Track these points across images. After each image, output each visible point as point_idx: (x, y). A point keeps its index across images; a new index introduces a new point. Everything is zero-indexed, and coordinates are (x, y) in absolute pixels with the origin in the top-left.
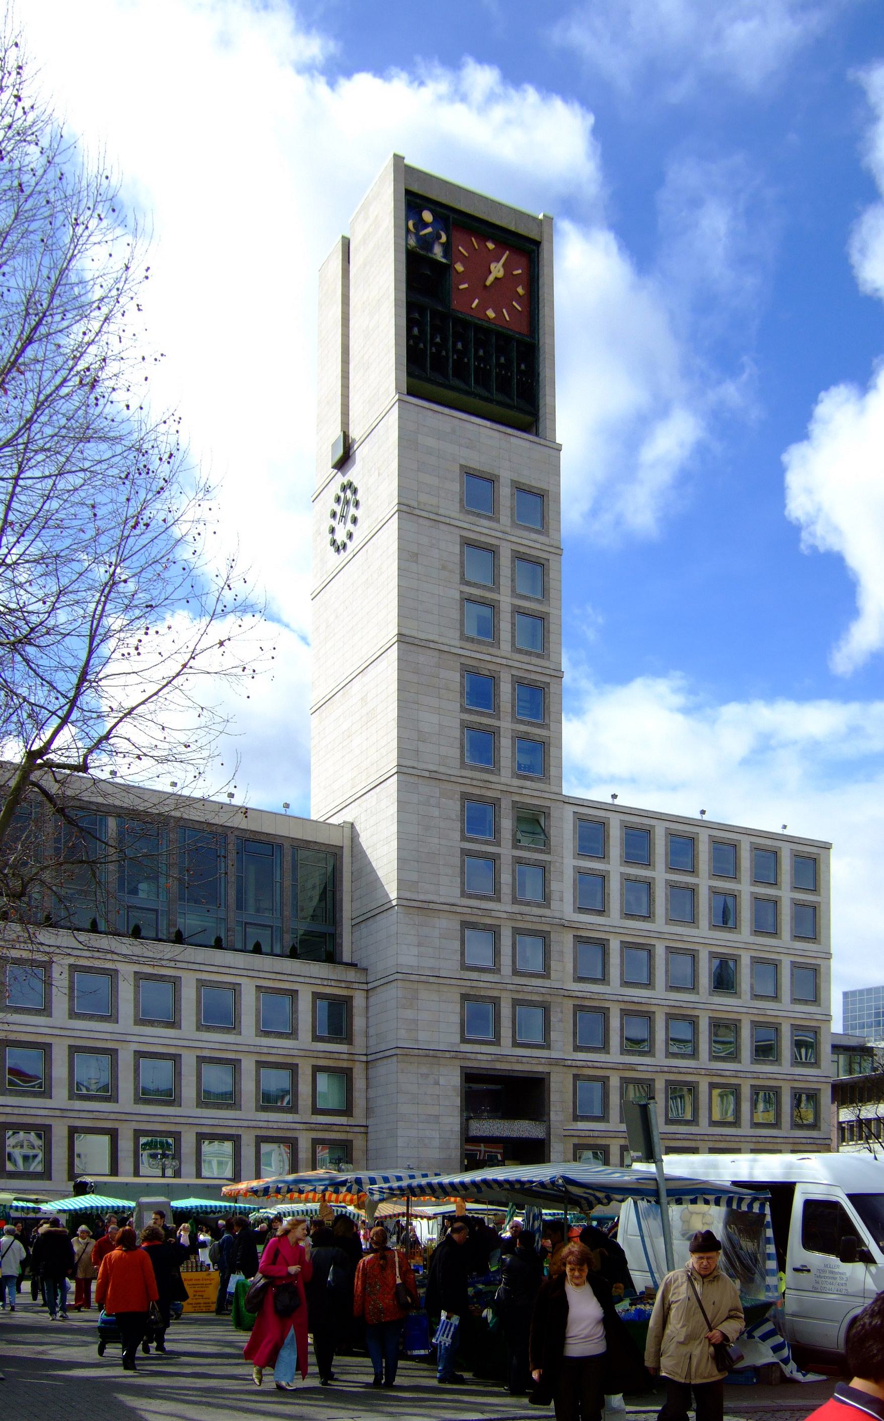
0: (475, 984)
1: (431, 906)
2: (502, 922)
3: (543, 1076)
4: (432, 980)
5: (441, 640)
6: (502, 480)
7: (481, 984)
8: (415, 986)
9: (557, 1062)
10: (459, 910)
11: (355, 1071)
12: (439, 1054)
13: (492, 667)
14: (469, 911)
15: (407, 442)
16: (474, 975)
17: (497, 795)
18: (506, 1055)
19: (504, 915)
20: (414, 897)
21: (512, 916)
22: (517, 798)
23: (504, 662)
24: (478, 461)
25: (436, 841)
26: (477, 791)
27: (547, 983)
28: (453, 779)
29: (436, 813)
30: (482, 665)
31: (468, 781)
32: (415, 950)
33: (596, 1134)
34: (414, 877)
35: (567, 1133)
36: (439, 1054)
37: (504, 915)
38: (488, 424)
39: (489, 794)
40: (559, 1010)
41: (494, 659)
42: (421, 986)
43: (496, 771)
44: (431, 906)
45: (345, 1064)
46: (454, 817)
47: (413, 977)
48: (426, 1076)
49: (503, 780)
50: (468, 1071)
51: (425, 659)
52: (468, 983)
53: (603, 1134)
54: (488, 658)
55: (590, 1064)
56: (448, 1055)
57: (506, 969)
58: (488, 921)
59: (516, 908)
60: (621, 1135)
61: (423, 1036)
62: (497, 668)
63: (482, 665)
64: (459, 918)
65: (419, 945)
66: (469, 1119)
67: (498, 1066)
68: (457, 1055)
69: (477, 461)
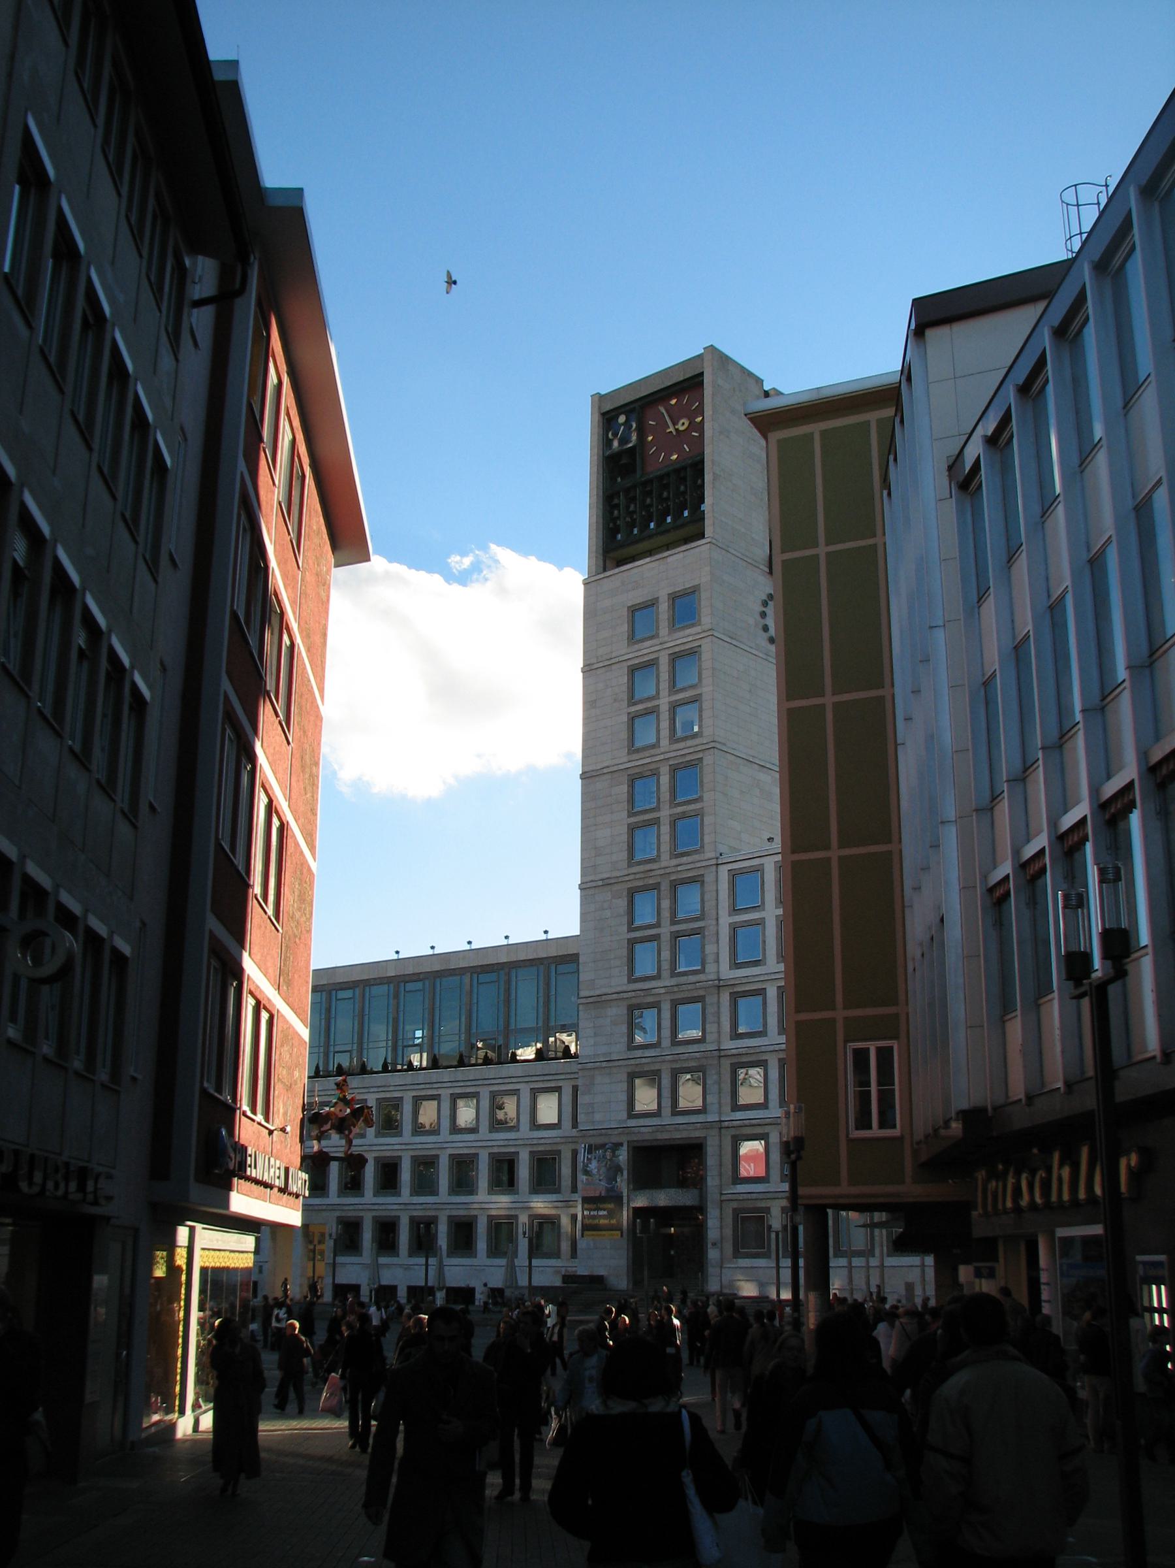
1: (604, 998)
4: (604, 1064)
6: (661, 600)
9: (707, 1125)
10: (625, 995)
13: (653, 766)
16: (639, 1053)
19: (662, 991)
20: (592, 994)
23: (662, 757)
26: (640, 883)
27: (702, 1047)
31: (631, 877)
33: (754, 1196)
35: (724, 1198)
36: (609, 1132)
38: (648, 560)
44: (604, 998)
49: (663, 864)
50: (636, 1144)
52: (632, 1062)
53: (761, 1196)
56: (616, 1132)
57: (666, 1042)
58: (650, 999)
59: (674, 981)
60: (780, 1195)
61: (598, 1117)
64: (625, 1003)
65: (596, 1035)
67: (660, 1136)
69: (637, 597)
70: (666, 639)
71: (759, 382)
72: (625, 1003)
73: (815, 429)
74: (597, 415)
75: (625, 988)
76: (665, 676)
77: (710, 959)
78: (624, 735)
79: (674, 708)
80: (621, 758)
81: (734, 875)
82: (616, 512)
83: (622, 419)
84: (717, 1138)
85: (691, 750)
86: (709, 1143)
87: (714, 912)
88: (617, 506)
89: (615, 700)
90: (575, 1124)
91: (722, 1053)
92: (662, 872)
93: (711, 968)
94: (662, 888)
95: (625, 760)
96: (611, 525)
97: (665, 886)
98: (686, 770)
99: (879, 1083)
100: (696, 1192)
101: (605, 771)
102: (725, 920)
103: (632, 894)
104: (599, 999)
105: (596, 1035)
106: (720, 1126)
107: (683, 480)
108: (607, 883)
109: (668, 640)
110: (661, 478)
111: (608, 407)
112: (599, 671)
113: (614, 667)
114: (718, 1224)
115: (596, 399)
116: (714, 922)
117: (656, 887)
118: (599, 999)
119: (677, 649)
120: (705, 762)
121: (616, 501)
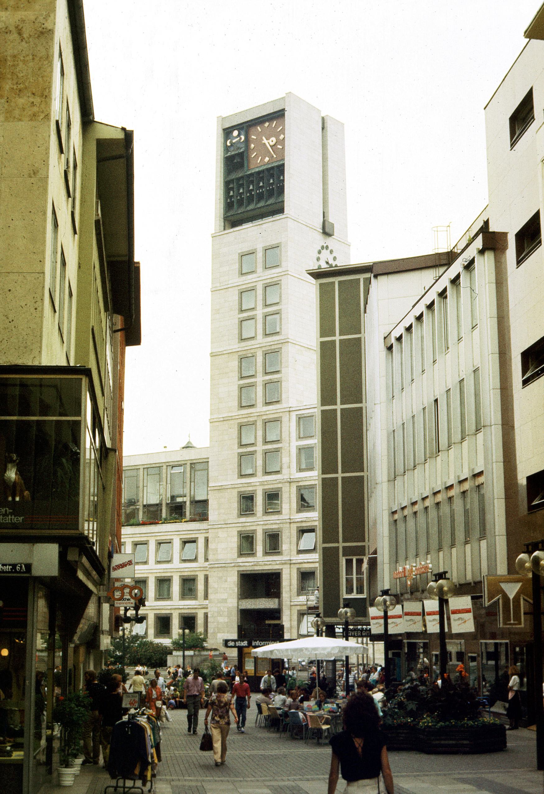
3: (278, 571)
4: (223, 526)
6: (258, 250)
8: (217, 530)
12: (227, 565)
13: (252, 351)
14: (241, 485)
18: (260, 562)
19: (258, 484)
21: (262, 483)
22: (265, 417)
23: (258, 346)
26: (246, 420)
28: (233, 418)
30: (249, 352)
31: (241, 416)
35: (292, 604)
36: (227, 565)
39: (251, 419)
40: (287, 531)
42: (220, 530)
48: (220, 578)
55: (306, 561)
69: (245, 248)
71: (319, 111)
72: (236, 490)
73: (336, 280)
74: (221, 132)
76: (260, 297)
77: (285, 466)
78: (236, 332)
79: (265, 316)
80: (236, 346)
81: (299, 418)
82: (231, 193)
83: (236, 133)
84: (289, 570)
86: (284, 573)
87: (287, 438)
88: (232, 189)
90: (207, 560)
91: (292, 521)
92: (258, 414)
93: (285, 471)
94: (258, 424)
95: (236, 346)
96: (229, 201)
97: (260, 424)
98: (272, 354)
99: (357, 574)
100: (276, 600)
101: (224, 352)
102: (295, 444)
103: (241, 427)
106: (290, 563)
107: (272, 176)
109: (263, 276)
110: (259, 173)
111: (227, 125)
113: (230, 289)
114: (289, 619)
115: (221, 120)
116: (288, 445)
117: (254, 423)
119: (268, 281)
120: (283, 350)
121: (231, 186)
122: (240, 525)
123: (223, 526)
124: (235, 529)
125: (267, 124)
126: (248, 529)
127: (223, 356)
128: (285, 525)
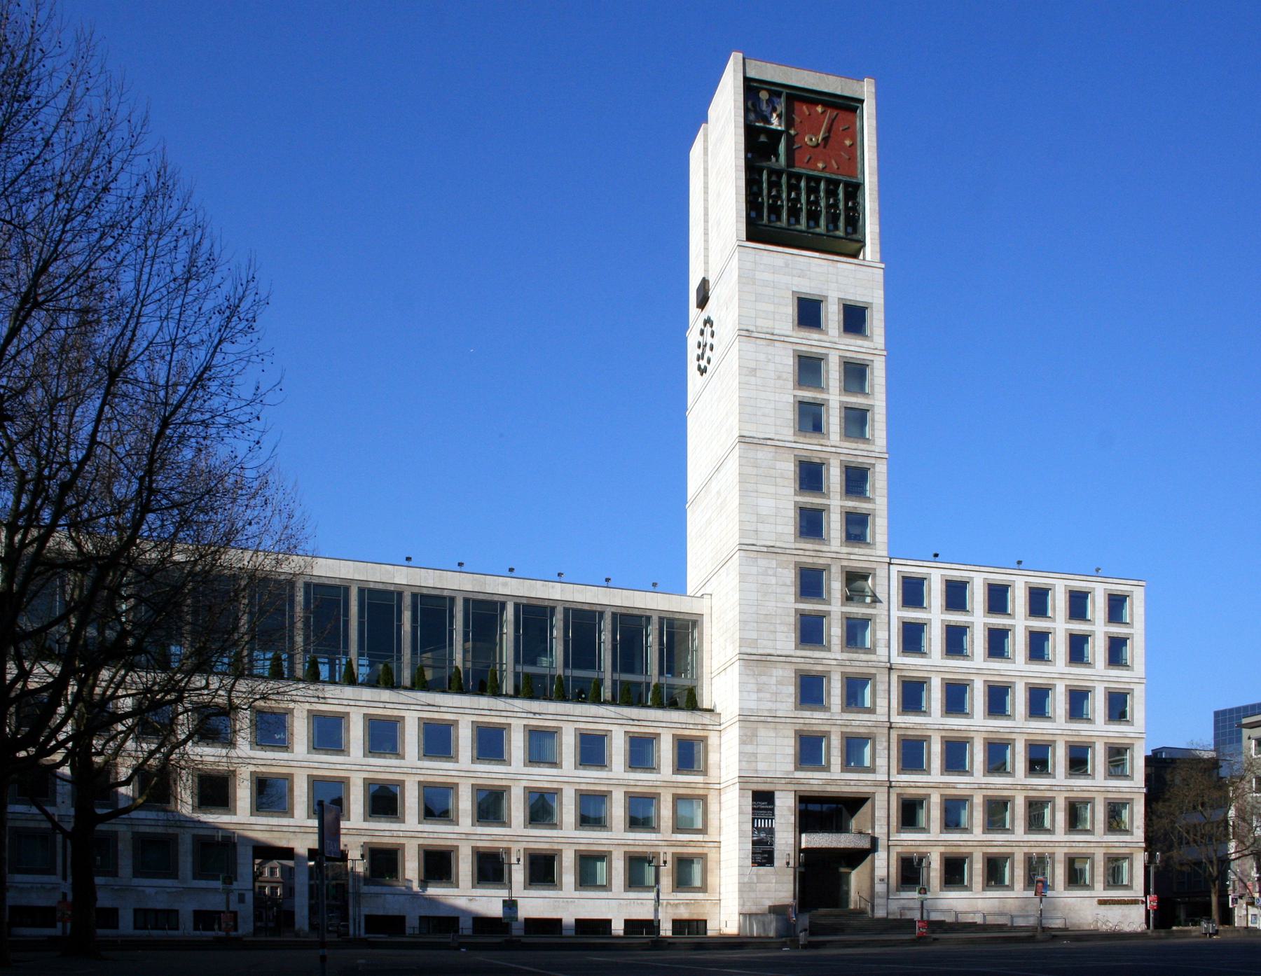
0: (807, 721)
2: (833, 668)
4: (769, 719)
5: (777, 437)
6: (830, 299)
7: (813, 721)
8: (755, 725)
11: (710, 798)
13: (822, 455)
15: (746, 279)
17: (829, 561)
22: (845, 563)
23: (833, 450)
24: (810, 288)
25: (773, 604)
27: (873, 717)
29: (773, 581)
32: (754, 696)
34: (754, 635)
37: (834, 662)
38: (817, 255)
41: (824, 449)
42: (760, 725)
43: (827, 542)
45: (701, 792)
46: (789, 583)
47: (752, 719)
49: (833, 549)
51: (764, 454)
52: (802, 721)
54: (819, 448)
56: (783, 781)
61: (761, 766)
62: (826, 456)
63: (815, 454)
65: (759, 691)
66: (800, 833)
67: (829, 788)
68: (790, 781)
70: (836, 340)
72: (793, 667)
75: (792, 653)
85: (865, 453)
89: (779, 378)
92: (834, 555)
93: (882, 651)
95: (792, 439)
104: (764, 658)
105: (759, 691)
108: (771, 551)
112: (758, 341)
113: (777, 344)
118: (764, 658)
122: (802, 721)
123: (769, 719)
124: (789, 726)
125: (819, 109)
126: (815, 728)
127: (766, 448)
128: (880, 730)
